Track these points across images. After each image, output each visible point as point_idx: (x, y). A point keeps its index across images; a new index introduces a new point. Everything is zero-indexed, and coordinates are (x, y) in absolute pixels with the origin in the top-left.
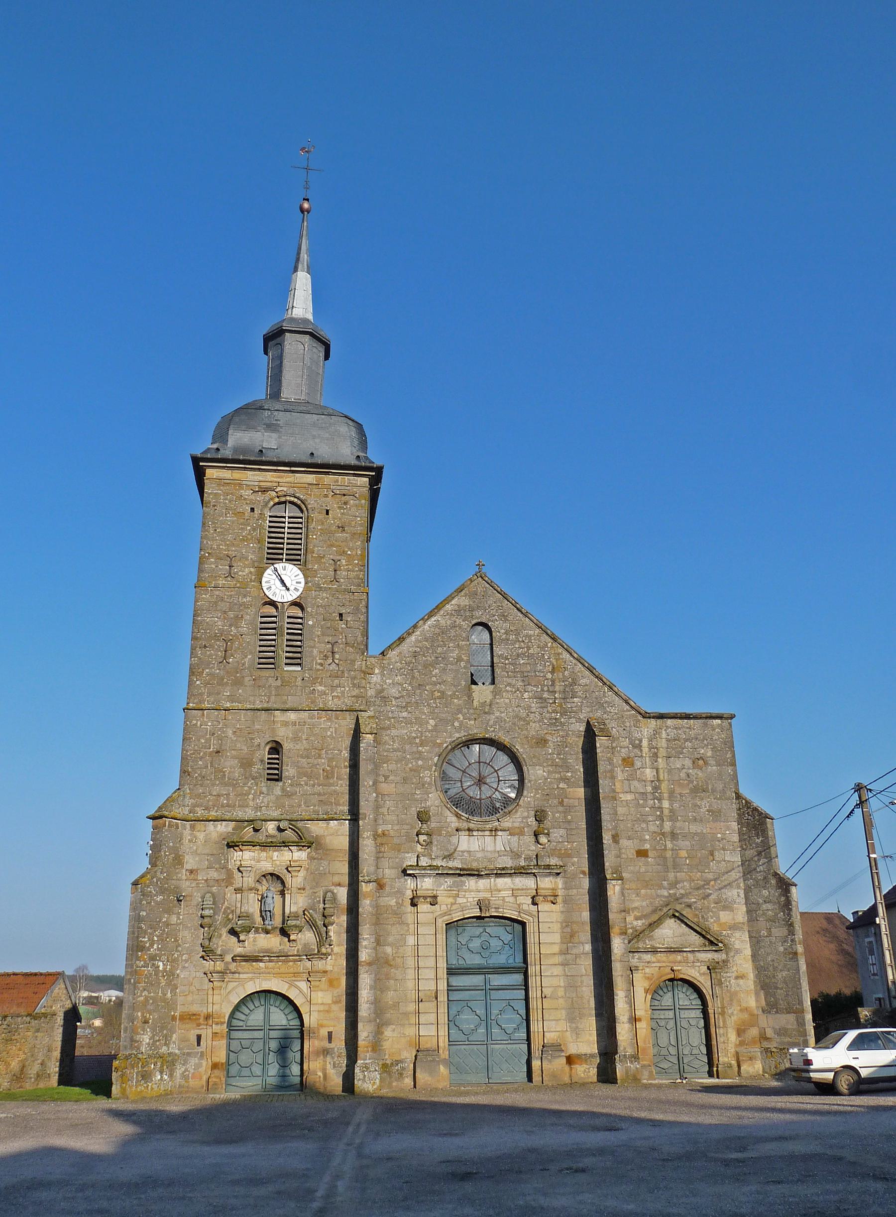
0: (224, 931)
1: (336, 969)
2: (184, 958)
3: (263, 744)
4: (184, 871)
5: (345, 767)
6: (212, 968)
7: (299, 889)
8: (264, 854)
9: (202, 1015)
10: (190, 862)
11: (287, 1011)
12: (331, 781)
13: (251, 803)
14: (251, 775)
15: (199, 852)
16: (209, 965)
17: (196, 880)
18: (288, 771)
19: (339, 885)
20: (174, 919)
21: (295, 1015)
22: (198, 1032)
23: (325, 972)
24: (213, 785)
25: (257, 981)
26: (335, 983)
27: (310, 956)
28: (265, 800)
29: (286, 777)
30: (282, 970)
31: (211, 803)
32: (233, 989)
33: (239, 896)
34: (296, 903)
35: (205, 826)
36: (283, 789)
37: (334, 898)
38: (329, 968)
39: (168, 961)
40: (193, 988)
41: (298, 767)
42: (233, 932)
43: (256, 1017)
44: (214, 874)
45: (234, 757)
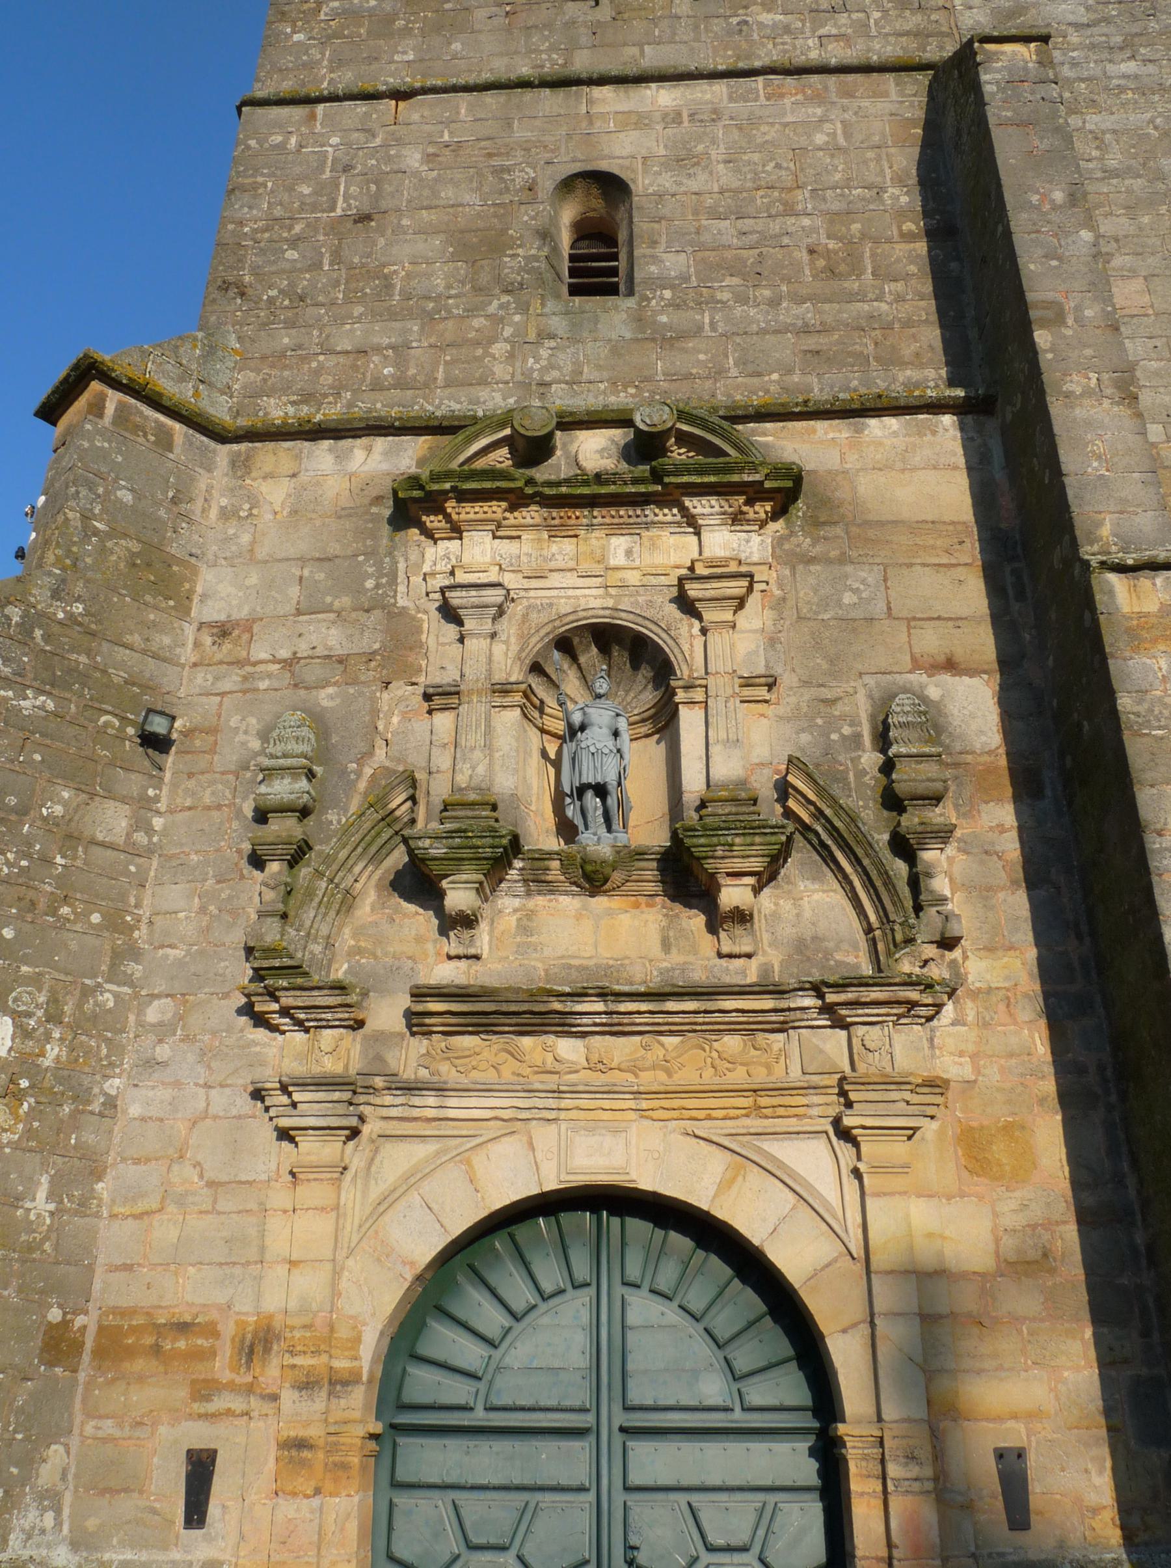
0: (369, 882)
1: (992, 1074)
2: (152, 1014)
3: (547, 185)
4: (190, 631)
5: (908, 237)
6: (294, 1068)
7: (748, 682)
8: (563, 549)
9: (228, 1330)
10: (220, 592)
11: (725, 1322)
12: (853, 285)
13: (500, 371)
14: (498, 279)
15: (261, 553)
16: (283, 1052)
17: (247, 662)
18: (655, 259)
19: (950, 665)
20: (112, 820)
21: (774, 1342)
22: (199, 1435)
23: (936, 1085)
24: (339, 321)
25: (546, 1136)
26: (999, 1151)
27: (836, 1000)
28: (565, 360)
29: (645, 281)
30: (687, 1076)
31: (327, 380)
32: (412, 1180)
33: (443, 721)
34: (733, 745)
35: (298, 457)
36: (639, 320)
37: (931, 721)
38: (952, 1068)
39: (54, 1017)
40: (185, 1175)
41: (702, 247)
42: (419, 883)
43: (545, 1344)
44: (329, 636)
45: (424, 231)
